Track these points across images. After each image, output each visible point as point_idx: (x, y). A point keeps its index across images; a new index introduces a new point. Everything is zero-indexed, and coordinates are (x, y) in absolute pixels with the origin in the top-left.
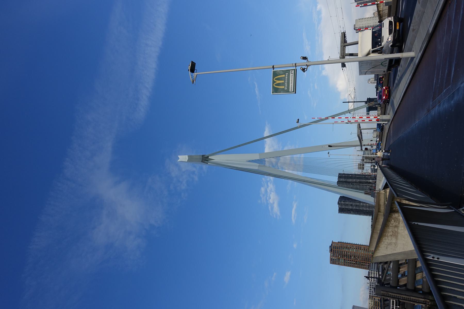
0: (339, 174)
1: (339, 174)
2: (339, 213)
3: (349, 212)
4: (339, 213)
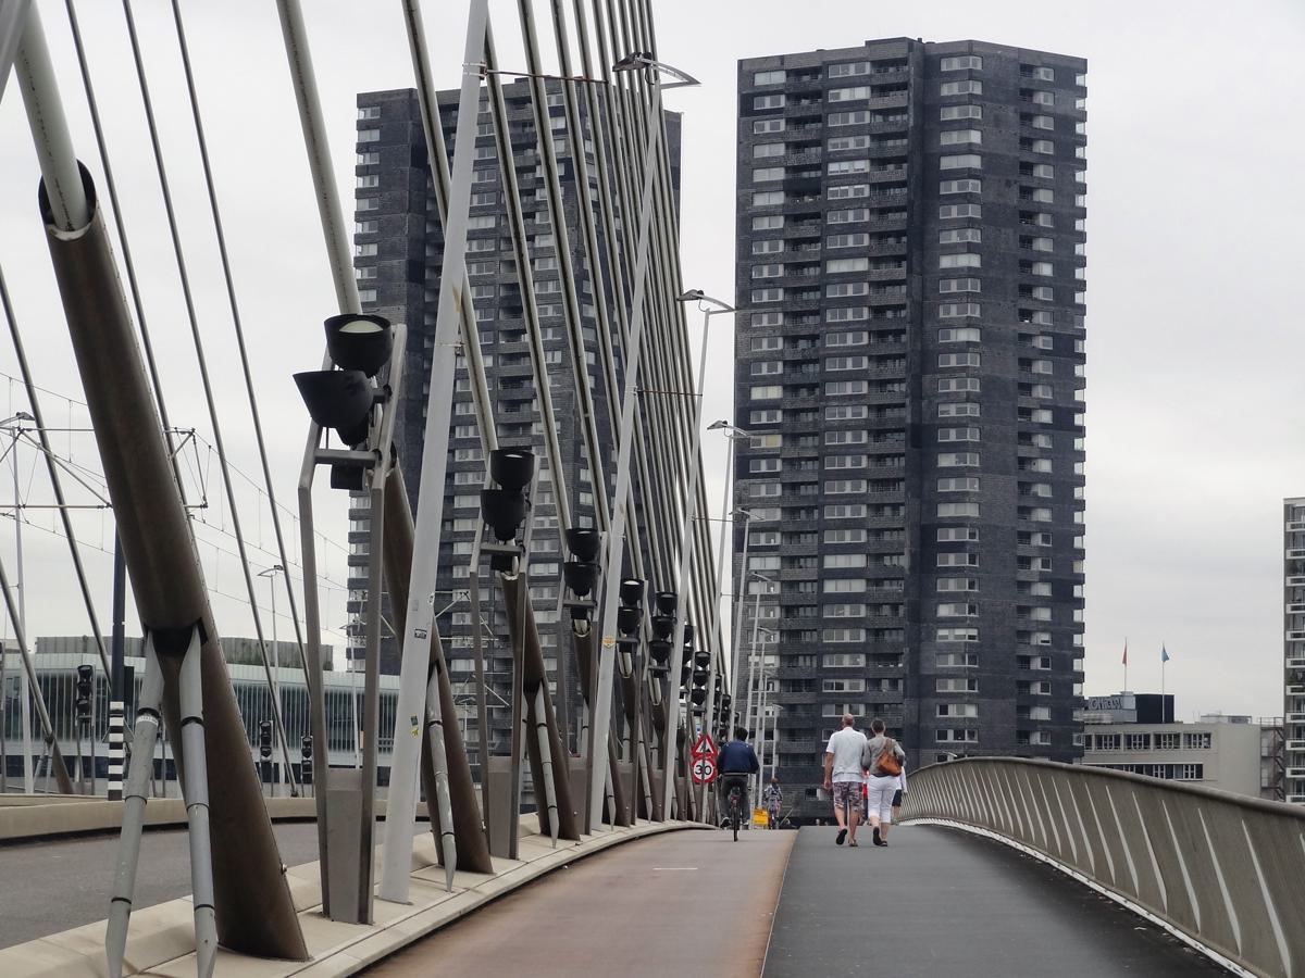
0: (1068, 72)
1: (1068, 72)
2: (364, 101)
3: (398, 265)
4: (364, 101)
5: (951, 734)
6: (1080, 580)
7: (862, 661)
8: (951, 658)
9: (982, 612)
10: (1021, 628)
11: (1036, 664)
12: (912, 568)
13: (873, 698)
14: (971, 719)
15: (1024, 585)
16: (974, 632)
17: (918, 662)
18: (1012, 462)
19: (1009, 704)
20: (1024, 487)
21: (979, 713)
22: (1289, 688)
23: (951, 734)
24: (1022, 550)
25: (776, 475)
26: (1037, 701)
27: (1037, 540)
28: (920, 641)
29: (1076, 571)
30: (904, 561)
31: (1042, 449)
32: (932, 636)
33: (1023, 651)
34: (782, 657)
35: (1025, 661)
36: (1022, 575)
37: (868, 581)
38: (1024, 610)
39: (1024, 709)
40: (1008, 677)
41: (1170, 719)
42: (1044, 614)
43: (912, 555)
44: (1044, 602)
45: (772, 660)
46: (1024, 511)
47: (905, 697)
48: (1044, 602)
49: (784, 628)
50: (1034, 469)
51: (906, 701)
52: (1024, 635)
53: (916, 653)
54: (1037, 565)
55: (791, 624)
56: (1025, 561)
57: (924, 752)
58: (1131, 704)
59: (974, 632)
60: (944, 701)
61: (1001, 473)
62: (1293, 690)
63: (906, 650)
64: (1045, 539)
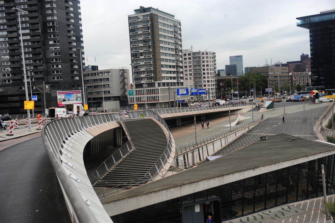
5: (55, 72)
6: (82, 37)
7: (31, 56)
8: (54, 54)
9: (60, 43)
10: (70, 47)
11: (74, 55)
12: (41, 32)
13: (35, 64)
14: (60, 68)
15: (70, 37)
16: (59, 47)
17: (46, 55)
18: (64, 8)
19: (69, 64)
20: (68, 14)
21: (62, 67)
22: (132, 58)
23: (55, 72)
24: (68, 29)
25: (3, 11)
26: (75, 64)
27: (72, 26)
28: (46, 50)
29: (81, 34)
30: (40, 31)
31: (71, 5)
32: (48, 49)
33: (71, 52)
34: (10, 56)
35: (71, 55)
36: (69, 35)
37: (30, 30)
38: (70, 43)
39: (72, 66)
40: (68, 58)
41: (98, 69)
42: (75, 44)
43: (41, 29)
44: (74, 41)
45: (8, 57)
46: (68, 19)
47: (43, 63)
48: (74, 41)
49: (10, 49)
50: (69, 9)
51: (43, 65)
52: (71, 49)
53: (45, 53)
54: (72, 32)
55: (12, 48)
56: (69, 31)
57: (49, 77)
58: (90, 67)
59: (59, 47)
60: (53, 64)
61: (62, 9)
62: (134, 58)
63: (42, 52)
64: (73, 26)
